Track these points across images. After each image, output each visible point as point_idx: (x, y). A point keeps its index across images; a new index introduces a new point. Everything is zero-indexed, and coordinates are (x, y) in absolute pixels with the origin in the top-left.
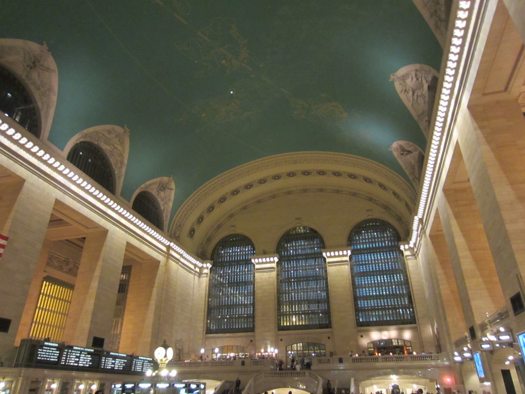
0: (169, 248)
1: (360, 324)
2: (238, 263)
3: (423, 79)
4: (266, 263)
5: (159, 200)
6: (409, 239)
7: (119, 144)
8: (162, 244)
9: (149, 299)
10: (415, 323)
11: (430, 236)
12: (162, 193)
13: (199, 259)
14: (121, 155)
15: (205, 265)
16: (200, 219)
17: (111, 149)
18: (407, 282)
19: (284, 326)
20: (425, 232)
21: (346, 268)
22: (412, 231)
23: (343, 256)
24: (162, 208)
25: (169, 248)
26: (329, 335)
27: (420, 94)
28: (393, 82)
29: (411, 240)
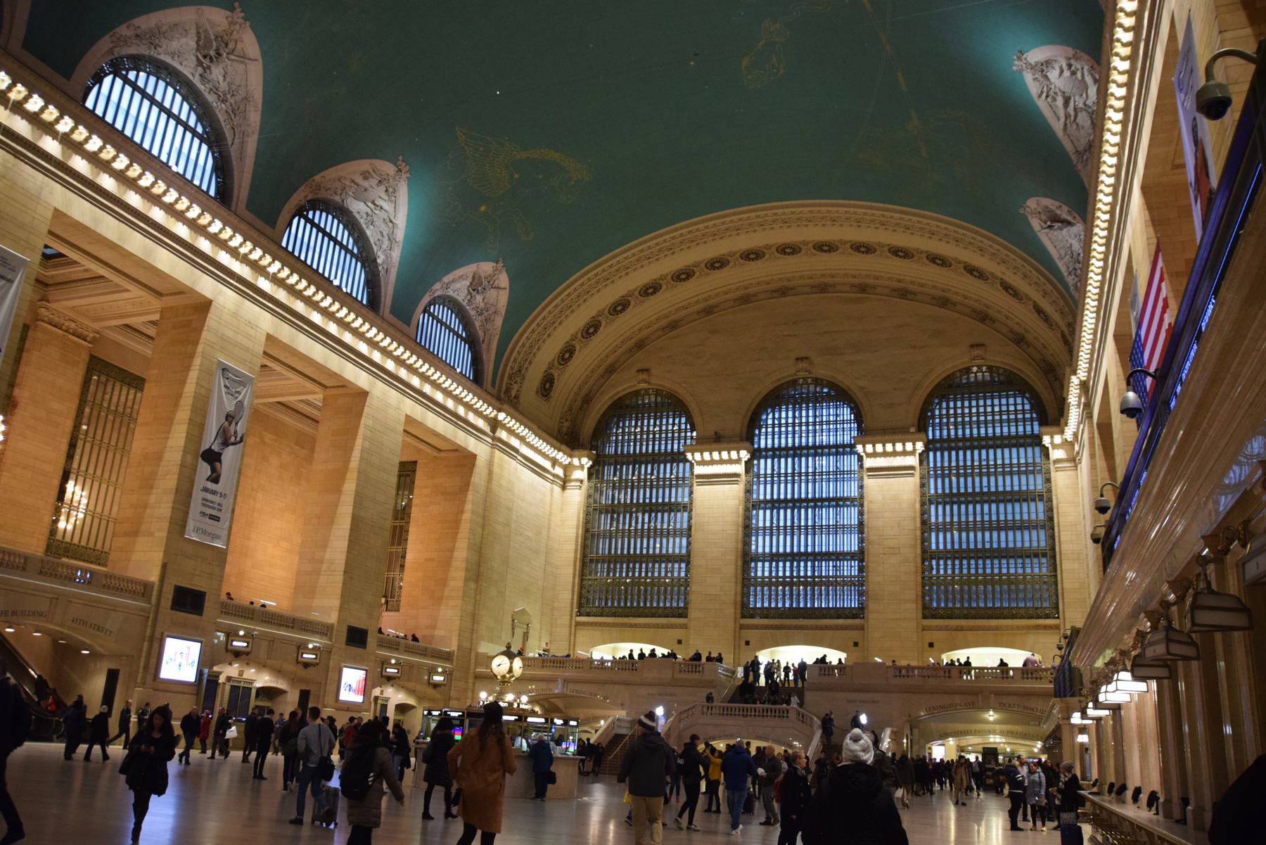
0: (495, 424)
2: (656, 459)
4: (721, 462)
5: (473, 313)
6: (1062, 421)
12: (479, 298)
13: (563, 447)
15: (576, 461)
16: (567, 354)
19: (755, 608)
23: (904, 453)
24: (481, 334)
25: (495, 424)
27: (1081, 105)
29: (1066, 424)
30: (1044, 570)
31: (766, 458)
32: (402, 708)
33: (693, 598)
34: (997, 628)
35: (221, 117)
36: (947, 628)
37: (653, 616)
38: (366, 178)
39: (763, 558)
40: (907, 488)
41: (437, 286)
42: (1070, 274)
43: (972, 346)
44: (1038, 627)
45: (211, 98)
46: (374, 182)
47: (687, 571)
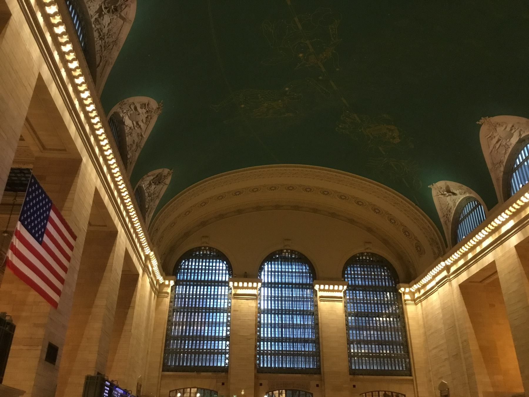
0: (147, 257)
3: (517, 131)
4: (247, 288)
5: (147, 194)
6: (413, 282)
7: (144, 121)
9: (123, 324)
12: (153, 186)
13: (164, 274)
15: (167, 282)
18: (403, 328)
20: (450, 281)
22: (426, 275)
23: (338, 291)
24: (147, 207)
26: (318, 383)
27: (504, 144)
28: (480, 126)
30: (402, 352)
35: (97, 48)
38: (141, 108)
40: (340, 306)
42: (444, 216)
45: (96, 34)
46: (144, 111)
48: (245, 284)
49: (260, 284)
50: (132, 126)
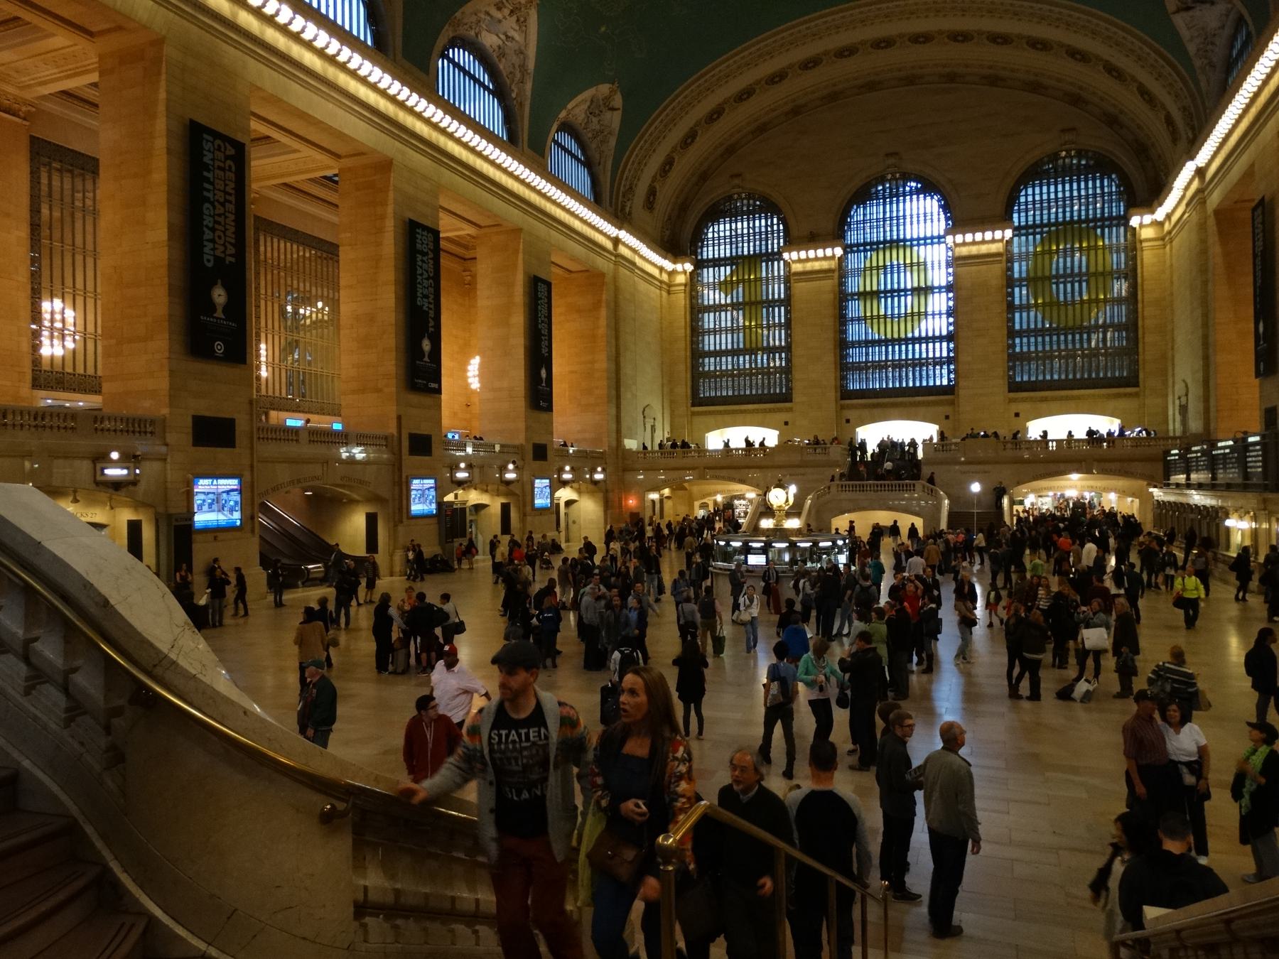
0: (616, 241)
1: (1014, 387)
4: (817, 259)
6: (1156, 203)
8: (605, 235)
10: (1136, 385)
11: (1217, 212)
12: (595, 120)
14: (520, 52)
15: (679, 267)
17: (500, 42)
20: (1203, 202)
21: (997, 269)
22: (1171, 189)
23: (993, 241)
24: (597, 156)
29: (1160, 205)
31: (858, 251)
32: (569, 503)
33: (798, 387)
34: (1078, 398)
36: (1031, 400)
37: (760, 402)
38: (499, 9)
39: (859, 344)
41: (563, 114)
43: (1063, 131)
44: (1118, 396)
47: (788, 360)
48: (811, 254)
49: (839, 251)
50: (500, 42)
